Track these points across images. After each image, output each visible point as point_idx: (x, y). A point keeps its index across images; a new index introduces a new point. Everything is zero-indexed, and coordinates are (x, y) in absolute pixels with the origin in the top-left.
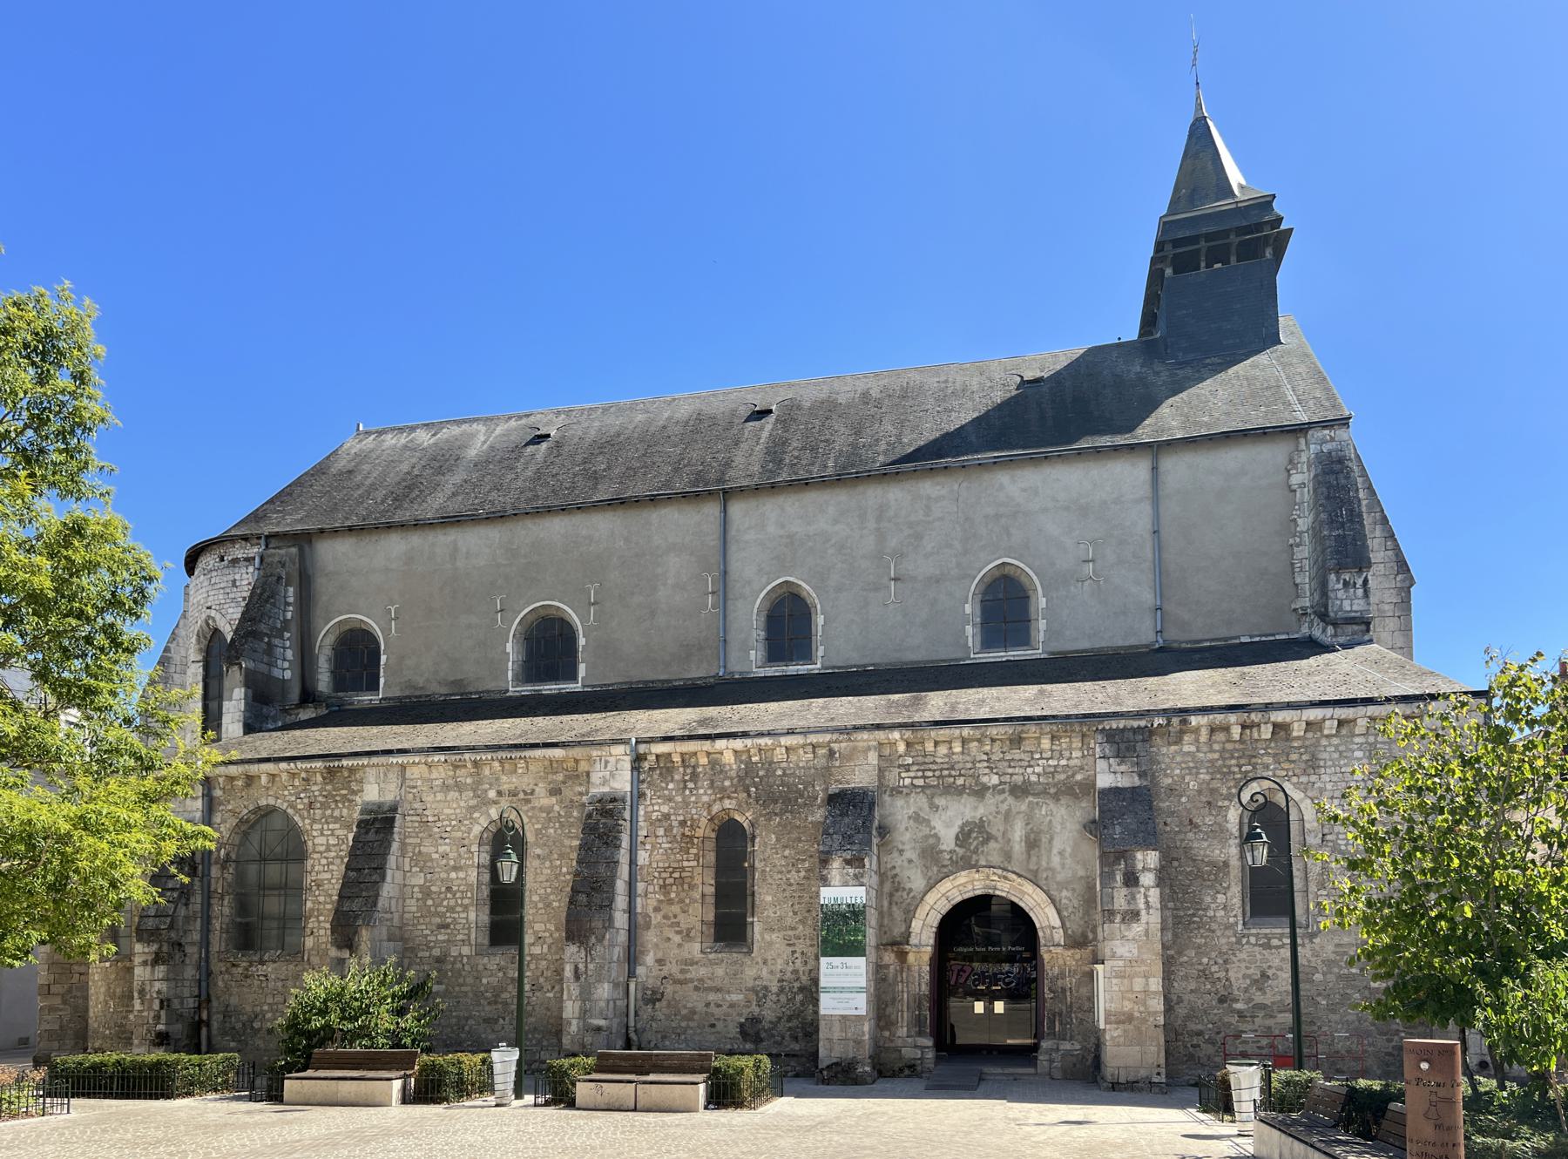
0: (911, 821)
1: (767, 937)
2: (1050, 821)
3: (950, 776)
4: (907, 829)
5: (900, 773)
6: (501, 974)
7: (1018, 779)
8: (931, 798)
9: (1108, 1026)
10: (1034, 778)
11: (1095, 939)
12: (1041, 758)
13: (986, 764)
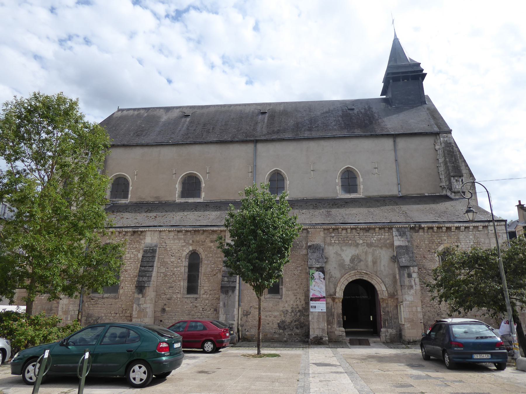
0: (335, 255)
1: (287, 293)
2: (380, 255)
3: (347, 240)
4: (333, 257)
5: (330, 239)
6: (191, 304)
7: (369, 242)
8: (341, 247)
9: (406, 323)
10: (374, 241)
11: (397, 294)
12: (376, 235)
13: (358, 237)
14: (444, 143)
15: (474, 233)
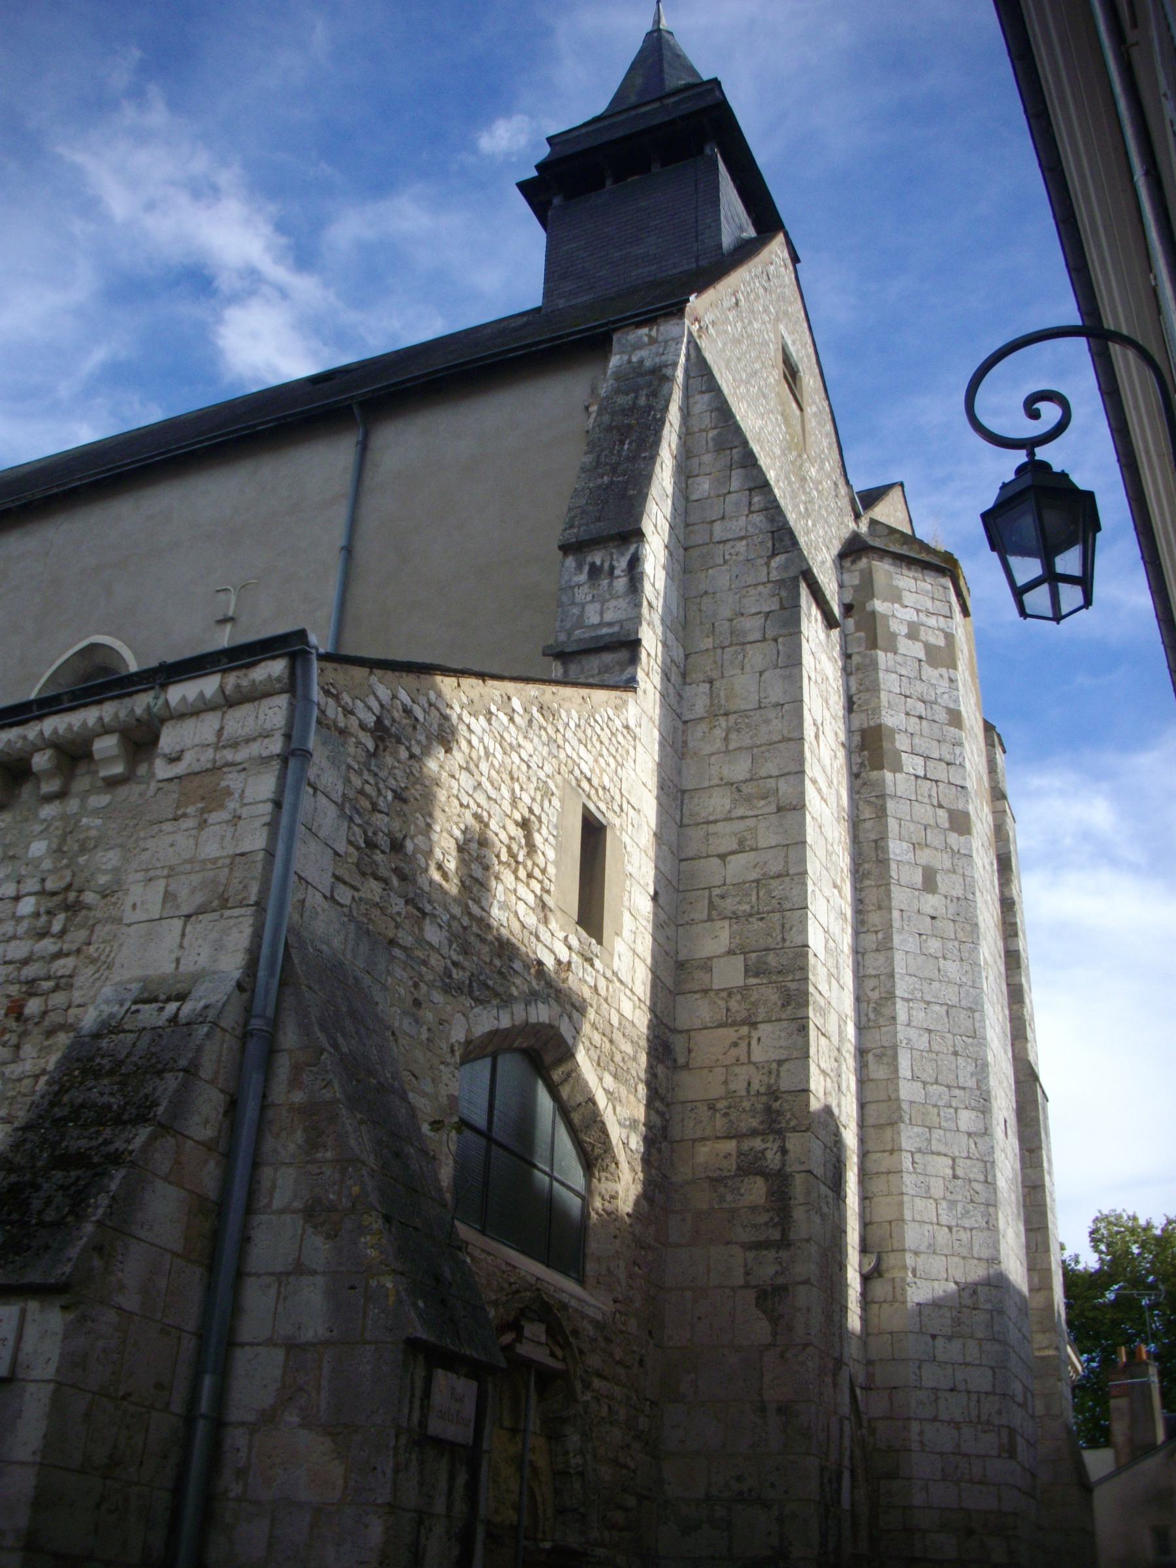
14: (617, 379)
15: (73, 805)
